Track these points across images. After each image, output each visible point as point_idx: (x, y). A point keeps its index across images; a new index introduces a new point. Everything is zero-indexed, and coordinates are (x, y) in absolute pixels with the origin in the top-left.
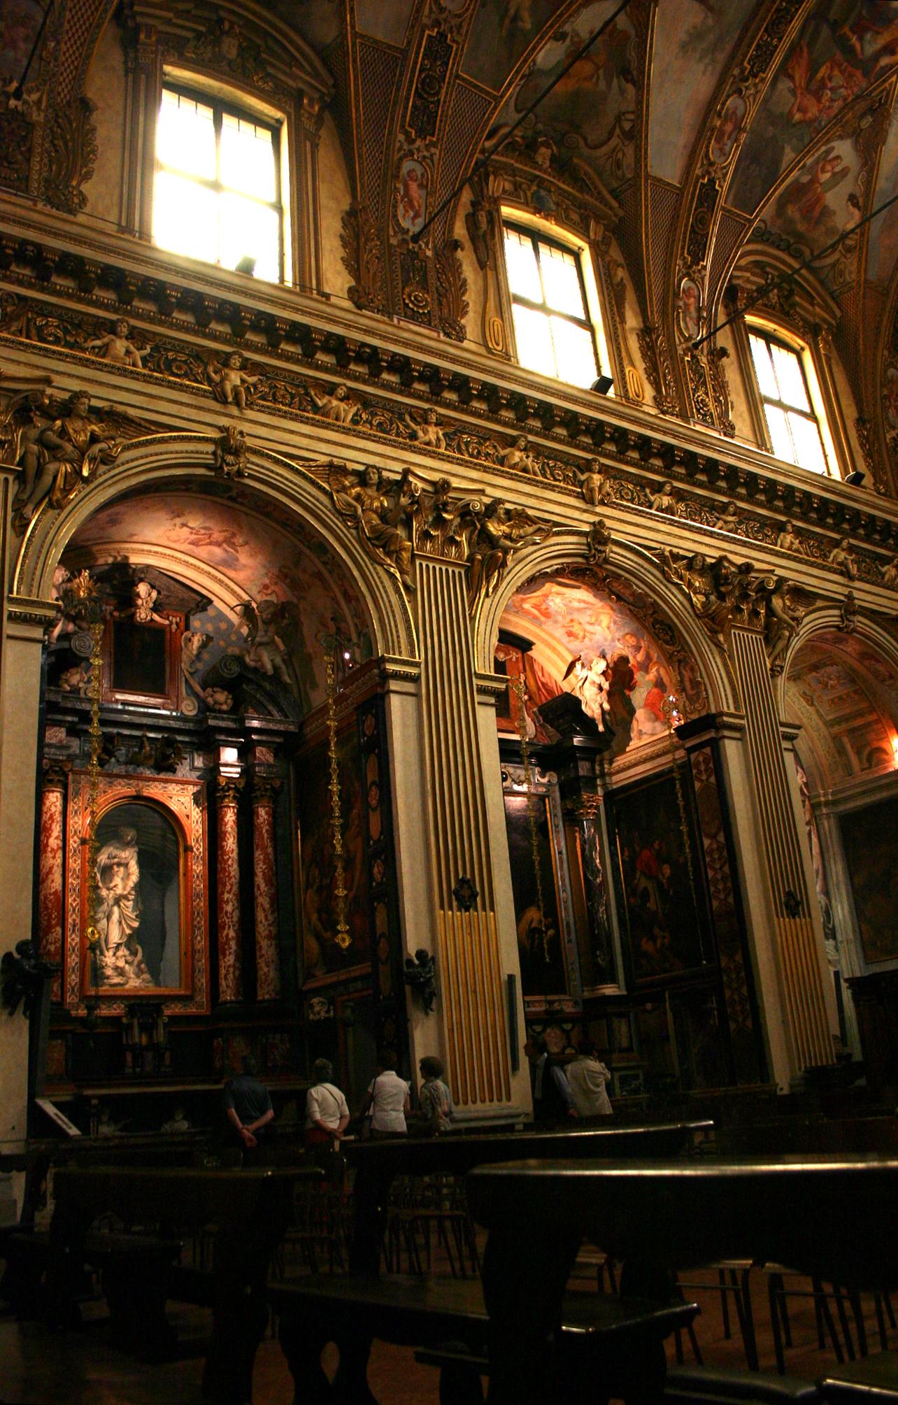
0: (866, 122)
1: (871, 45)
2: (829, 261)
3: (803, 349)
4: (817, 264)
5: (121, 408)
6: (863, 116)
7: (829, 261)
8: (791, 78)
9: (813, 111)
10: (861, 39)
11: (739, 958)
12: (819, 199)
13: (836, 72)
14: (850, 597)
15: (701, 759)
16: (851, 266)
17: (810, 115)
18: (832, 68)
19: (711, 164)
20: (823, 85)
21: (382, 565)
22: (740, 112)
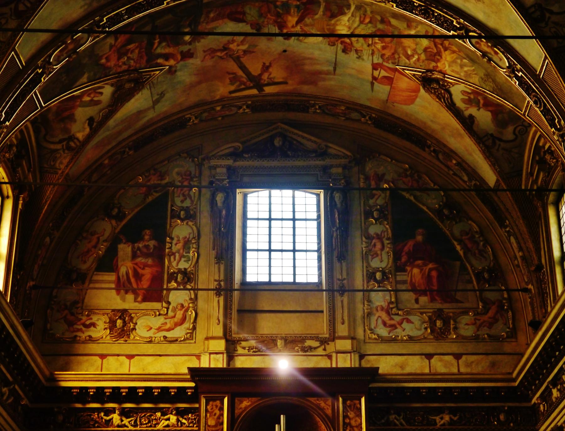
2: (52, 147)
3: (8, 197)
6: (129, 81)
7: (52, 147)
8: (116, 39)
9: (112, 63)
10: (160, 43)
12: (74, 107)
13: (137, 51)
18: (137, 48)
19: (50, 63)
20: (126, 54)
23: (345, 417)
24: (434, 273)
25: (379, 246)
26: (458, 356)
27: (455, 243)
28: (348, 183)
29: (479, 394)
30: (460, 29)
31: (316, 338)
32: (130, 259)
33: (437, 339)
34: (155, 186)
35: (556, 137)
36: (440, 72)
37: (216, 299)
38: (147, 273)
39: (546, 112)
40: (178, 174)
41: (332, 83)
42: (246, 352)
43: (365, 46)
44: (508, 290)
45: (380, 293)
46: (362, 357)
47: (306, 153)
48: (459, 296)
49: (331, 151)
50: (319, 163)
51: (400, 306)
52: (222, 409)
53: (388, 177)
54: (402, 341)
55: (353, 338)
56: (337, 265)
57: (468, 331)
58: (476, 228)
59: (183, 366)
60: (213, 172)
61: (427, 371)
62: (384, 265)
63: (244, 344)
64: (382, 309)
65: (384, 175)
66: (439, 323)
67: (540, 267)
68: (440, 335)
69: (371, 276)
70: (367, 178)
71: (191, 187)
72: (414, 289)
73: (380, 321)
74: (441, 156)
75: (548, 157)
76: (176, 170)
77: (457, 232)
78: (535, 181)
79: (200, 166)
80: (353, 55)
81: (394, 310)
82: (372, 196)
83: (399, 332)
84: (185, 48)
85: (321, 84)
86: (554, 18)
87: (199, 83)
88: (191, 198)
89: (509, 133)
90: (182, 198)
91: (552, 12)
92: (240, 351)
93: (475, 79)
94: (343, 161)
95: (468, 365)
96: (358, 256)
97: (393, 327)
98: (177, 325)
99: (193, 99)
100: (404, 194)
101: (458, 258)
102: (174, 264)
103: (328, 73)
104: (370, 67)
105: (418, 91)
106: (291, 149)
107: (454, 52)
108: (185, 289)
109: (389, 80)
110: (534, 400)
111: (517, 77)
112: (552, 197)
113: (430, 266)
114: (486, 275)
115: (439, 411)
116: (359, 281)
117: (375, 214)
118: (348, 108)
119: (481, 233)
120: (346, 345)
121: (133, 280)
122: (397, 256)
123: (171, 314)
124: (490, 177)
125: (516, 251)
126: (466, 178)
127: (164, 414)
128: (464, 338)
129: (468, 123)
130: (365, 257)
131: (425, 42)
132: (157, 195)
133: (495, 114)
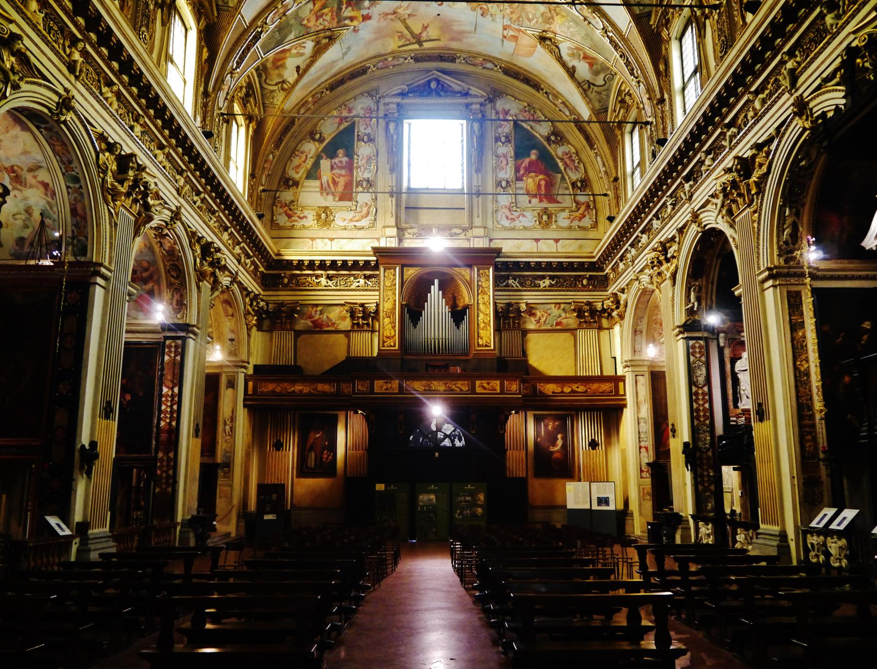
0: (325, 41)
1: (347, 12)
2: (271, 88)
4: (265, 86)
5: (28, 53)
6: (325, 38)
8: (314, 4)
9: (311, 24)
10: (346, 8)
11: (171, 455)
12: (284, 58)
13: (330, 14)
14: (237, 273)
15: (173, 344)
16: (279, 97)
17: (309, 25)
19: (266, 23)
20: (321, 16)
21: (108, 205)
22: (289, 7)
24: (543, 183)
25: (504, 162)
26: (557, 241)
27: (558, 161)
28: (483, 116)
29: (571, 266)
33: (543, 228)
34: (346, 118)
35: (634, 83)
36: (552, 32)
37: (390, 199)
38: (342, 181)
39: (628, 64)
40: (362, 108)
43: (498, 11)
44: (593, 195)
46: (491, 240)
47: (454, 93)
48: (559, 198)
49: (471, 92)
50: (463, 101)
52: (395, 275)
53: (512, 112)
54: (519, 229)
56: (475, 176)
57: (565, 223)
58: (573, 150)
61: (535, 250)
62: (507, 176)
63: (409, 231)
65: (509, 110)
66: (545, 218)
67: (616, 179)
68: (546, 225)
69: (499, 184)
70: (497, 113)
71: (371, 118)
72: (528, 194)
73: (504, 216)
74: (550, 97)
75: (627, 98)
76: (360, 106)
78: (618, 116)
79: (378, 102)
80: (489, 18)
81: (514, 208)
82: (501, 126)
83: (517, 223)
84: (365, 12)
85: (465, 40)
87: (376, 39)
89: (600, 81)
92: (407, 236)
93: (578, 38)
94: (481, 100)
95: (563, 247)
98: (363, 217)
99: (372, 52)
100: (523, 124)
101: (560, 172)
102: (360, 174)
103: (470, 32)
104: (502, 28)
105: (536, 47)
106: (442, 90)
107: (563, 16)
108: (368, 192)
109: (515, 38)
111: (608, 36)
112: (629, 127)
113: (541, 177)
114: (579, 184)
115: (543, 277)
116: (490, 188)
117: (503, 139)
118: (484, 60)
120: (480, 232)
121: (332, 186)
122: (517, 170)
124: (585, 112)
126: (568, 113)
127: (355, 278)
128: (562, 228)
129: (571, 72)
130: (494, 170)
133: (591, 65)
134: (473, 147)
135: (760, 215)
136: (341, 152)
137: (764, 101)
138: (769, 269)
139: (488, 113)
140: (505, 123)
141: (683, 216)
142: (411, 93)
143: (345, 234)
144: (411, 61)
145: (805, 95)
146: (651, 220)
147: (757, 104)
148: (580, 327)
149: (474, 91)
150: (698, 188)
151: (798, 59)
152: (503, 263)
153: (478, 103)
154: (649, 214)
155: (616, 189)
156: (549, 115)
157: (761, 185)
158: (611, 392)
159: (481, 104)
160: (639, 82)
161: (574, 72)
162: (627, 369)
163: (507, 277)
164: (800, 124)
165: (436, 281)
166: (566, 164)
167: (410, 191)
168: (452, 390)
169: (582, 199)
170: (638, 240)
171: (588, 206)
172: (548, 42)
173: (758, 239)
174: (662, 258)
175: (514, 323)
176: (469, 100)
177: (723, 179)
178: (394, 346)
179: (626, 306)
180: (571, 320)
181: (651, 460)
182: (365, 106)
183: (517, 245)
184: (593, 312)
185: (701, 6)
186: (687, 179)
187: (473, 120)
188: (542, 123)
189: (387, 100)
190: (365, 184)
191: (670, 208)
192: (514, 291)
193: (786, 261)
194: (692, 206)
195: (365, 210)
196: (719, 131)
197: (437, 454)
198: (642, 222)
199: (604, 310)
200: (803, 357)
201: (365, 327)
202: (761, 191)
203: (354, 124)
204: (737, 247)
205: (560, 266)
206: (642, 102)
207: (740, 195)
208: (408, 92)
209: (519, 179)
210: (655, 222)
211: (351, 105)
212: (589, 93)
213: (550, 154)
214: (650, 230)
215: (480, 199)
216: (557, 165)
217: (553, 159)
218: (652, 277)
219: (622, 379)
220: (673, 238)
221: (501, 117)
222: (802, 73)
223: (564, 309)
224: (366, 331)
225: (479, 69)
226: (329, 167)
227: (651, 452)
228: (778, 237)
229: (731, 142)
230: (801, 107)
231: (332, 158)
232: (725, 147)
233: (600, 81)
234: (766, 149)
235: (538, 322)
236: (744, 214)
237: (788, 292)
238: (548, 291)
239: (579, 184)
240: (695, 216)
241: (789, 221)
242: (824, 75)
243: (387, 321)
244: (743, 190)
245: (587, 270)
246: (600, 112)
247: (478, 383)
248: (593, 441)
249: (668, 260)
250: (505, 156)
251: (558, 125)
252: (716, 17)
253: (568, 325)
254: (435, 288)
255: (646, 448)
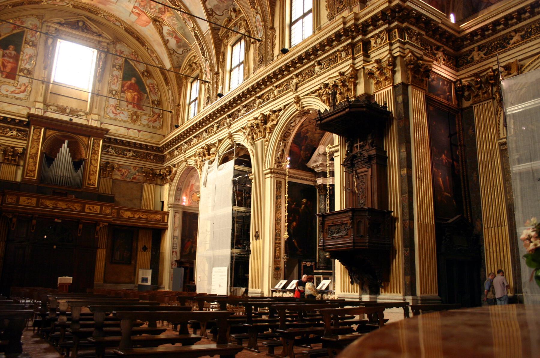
23: (93, 146)
24: (136, 97)
25: (116, 80)
26: (139, 131)
27: (147, 87)
28: (108, 51)
30: (178, 6)
31: (84, 112)
32: (1, 56)
33: (132, 122)
34: (19, 26)
37: (41, 85)
38: (9, 66)
39: (202, 49)
40: (31, 24)
41: (113, 7)
42: (52, 111)
45: (113, 100)
46: (101, 123)
47: (93, 33)
48: (144, 108)
49: (103, 35)
50: (97, 38)
51: (120, 106)
52: (40, 133)
53: (125, 53)
55: (99, 115)
56: (97, 84)
57: (145, 122)
58: (156, 83)
59: (25, 112)
60: (48, 28)
61: (126, 134)
62: (116, 88)
63: (51, 107)
64: (113, 106)
66: (135, 117)
68: (134, 121)
69: (111, 92)
70: (116, 51)
71: (37, 32)
72: (127, 101)
73: (111, 111)
74: (149, 51)
75: (194, 65)
76: (30, 22)
77: (148, 83)
78: (185, 72)
79: (42, 23)
81: (118, 108)
82: (117, 59)
85: (108, 6)
86: (216, 16)
88: (35, 37)
89: (180, 51)
90: (31, 36)
91: (216, 14)
92: (49, 110)
93: (176, 27)
95: (143, 135)
96: (107, 82)
97: (116, 114)
98: (21, 92)
100: (130, 62)
101: (147, 93)
102: (23, 65)
103: (113, 3)
104: (132, 7)
105: (149, 23)
106: (86, 29)
108: (27, 77)
109: (139, 15)
110: (166, 153)
111: (195, 32)
112: (191, 80)
113: (135, 93)
114: (156, 103)
115: (129, 151)
116: (105, 93)
118: (116, 20)
119: (157, 86)
120: (96, 117)
122: (123, 86)
123: (18, 86)
124: (168, 65)
125: (170, 96)
126: (157, 63)
127: (10, 130)
129: (166, 42)
130: (109, 83)
131: (161, 6)
132: (19, 31)
133: (178, 42)
134: (99, 66)
135: (269, 143)
136: (11, 47)
137: (279, 92)
138: (271, 169)
139: (111, 50)
140: (120, 58)
141: (224, 133)
142: (66, 24)
143: (7, 100)
144: (71, 6)
145: (300, 96)
146: (202, 132)
147: (276, 92)
148: (146, 181)
149: (105, 34)
150: (235, 123)
151: (300, 79)
152: (108, 138)
153: (105, 42)
154: (201, 128)
155: (178, 110)
156: (146, 61)
157: (271, 129)
158: (160, 220)
159: (108, 44)
160: (206, 60)
161: (168, 42)
162: (170, 209)
163: (109, 147)
164: (296, 107)
165: (66, 142)
166: (150, 89)
167: (54, 83)
168: (71, 209)
169: (156, 111)
170: (191, 140)
171: (159, 116)
172: (158, 23)
173: (266, 154)
174: (206, 153)
175: (109, 174)
176: (101, 39)
177: (252, 122)
178: (34, 177)
179: (176, 174)
180: (140, 177)
181: (178, 259)
182: (33, 23)
183: (117, 130)
184: (155, 175)
185: (250, 37)
186: (229, 116)
187: (102, 51)
188: (141, 64)
189: (49, 24)
190: (25, 72)
191: (215, 129)
192: (111, 155)
193: (278, 166)
194: (230, 130)
195: (23, 88)
196: (253, 98)
197: (55, 247)
198: (196, 132)
199: (160, 175)
200: (280, 211)
201: (13, 162)
202: (271, 132)
203: (23, 32)
204: (253, 155)
205: (141, 146)
206: (206, 71)
207: (259, 131)
208: (64, 24)
209: (123, 92)
210: (204, 133)
211: (24, 20)
212: (173, 56)
213: (143, 82)
214: (199, 137)
215: (99, 98)
216: (145, 89)
217: (144, 85)
218: (196, 162)
219: (167, 214)
220: (215, 143)
221: (118, 54)
222: (301, 86)
223: (138, 171)
224: (13, 164)
225: (111, 24)
226: (1, 55)
227: (178, 254)
228: (276, 155)
229: (259, 105)
230: (298, 100)
231: (4, 49)
232: (254, 107)
233: (180, 51)
234: (277, 113)
235: (122, 175)
236: (260, 141)
237: (277, 181)
238: (131, 159)
239: (156, 103)
240: (230, 136)
241: (281, 149)
242: (311, 90)
243: (31, 160)
244: (262, 129)
245: (154, 151)
246: (177, 67)
247: (87, 206)
248: (145, 246)
249: (209, 154)
250: (117, 77)
251: (150, 67)
252: (258, 45)
253: (139, 180)
254: (65, 146)
255: (176, 252)
